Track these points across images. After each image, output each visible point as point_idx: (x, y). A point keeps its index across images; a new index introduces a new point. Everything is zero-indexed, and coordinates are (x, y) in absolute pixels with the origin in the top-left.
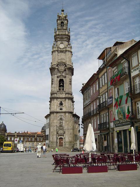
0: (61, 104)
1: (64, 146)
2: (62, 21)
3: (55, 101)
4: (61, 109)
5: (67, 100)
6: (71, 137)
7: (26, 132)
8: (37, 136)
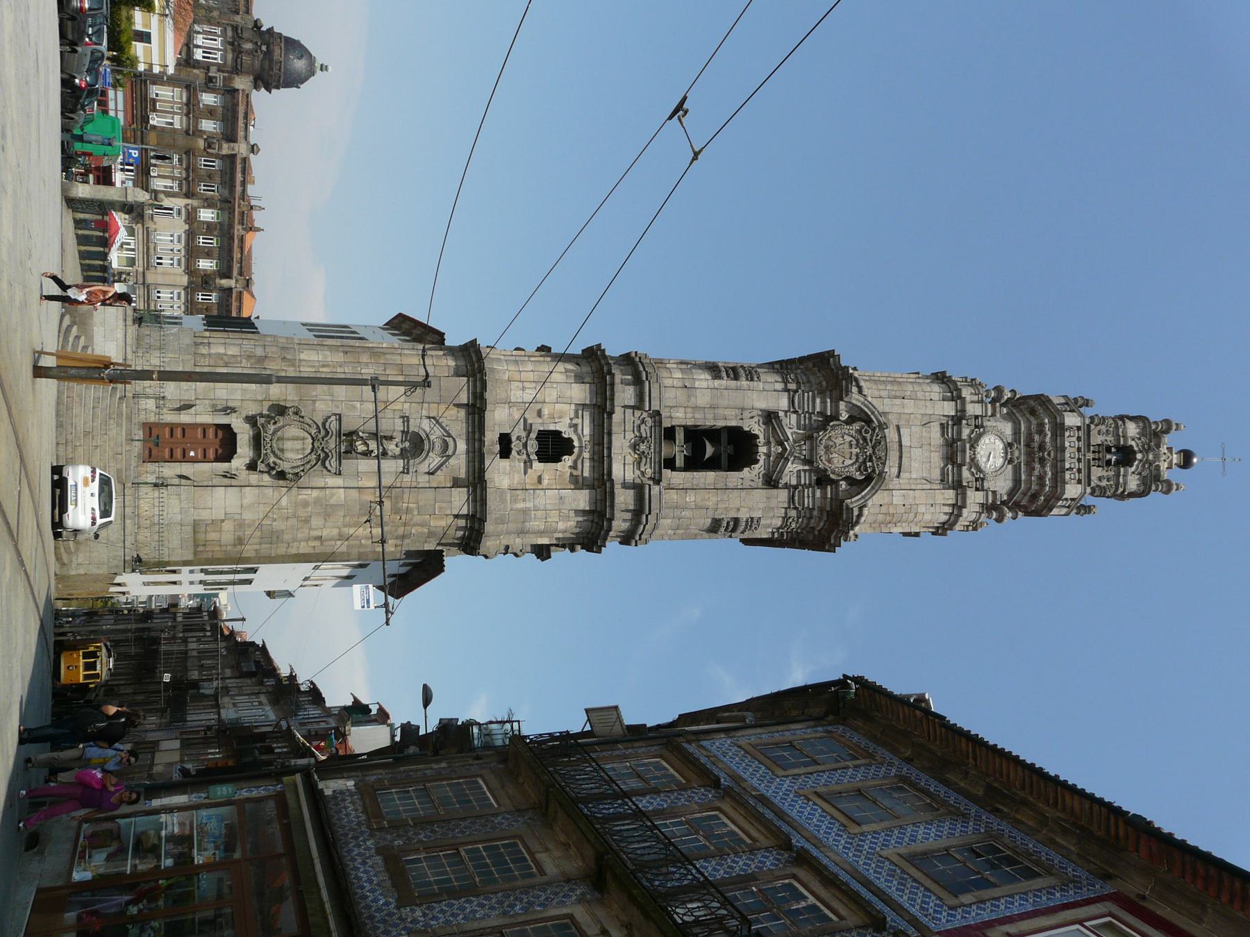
0: (552, 446)
1: (151, 472)
2: (1139, 456)
3: (581, 393)
4: (505, 443)
5: (582, 499)
6: (240, 541)
7: (258, 218)
8: (231, 289)
